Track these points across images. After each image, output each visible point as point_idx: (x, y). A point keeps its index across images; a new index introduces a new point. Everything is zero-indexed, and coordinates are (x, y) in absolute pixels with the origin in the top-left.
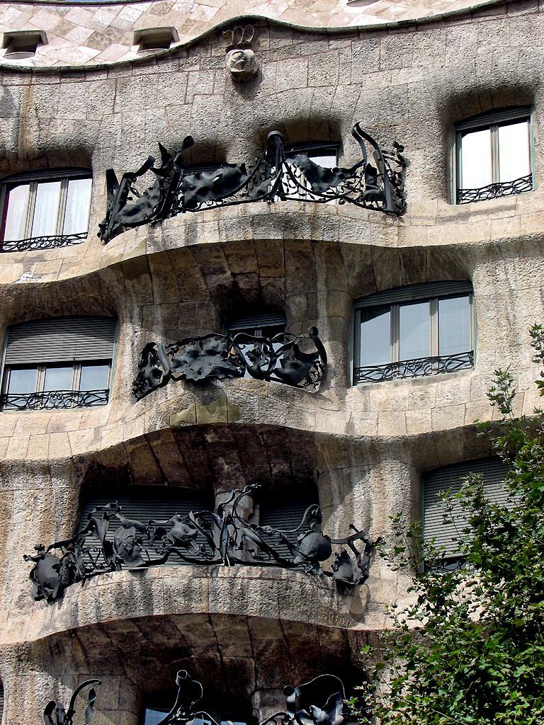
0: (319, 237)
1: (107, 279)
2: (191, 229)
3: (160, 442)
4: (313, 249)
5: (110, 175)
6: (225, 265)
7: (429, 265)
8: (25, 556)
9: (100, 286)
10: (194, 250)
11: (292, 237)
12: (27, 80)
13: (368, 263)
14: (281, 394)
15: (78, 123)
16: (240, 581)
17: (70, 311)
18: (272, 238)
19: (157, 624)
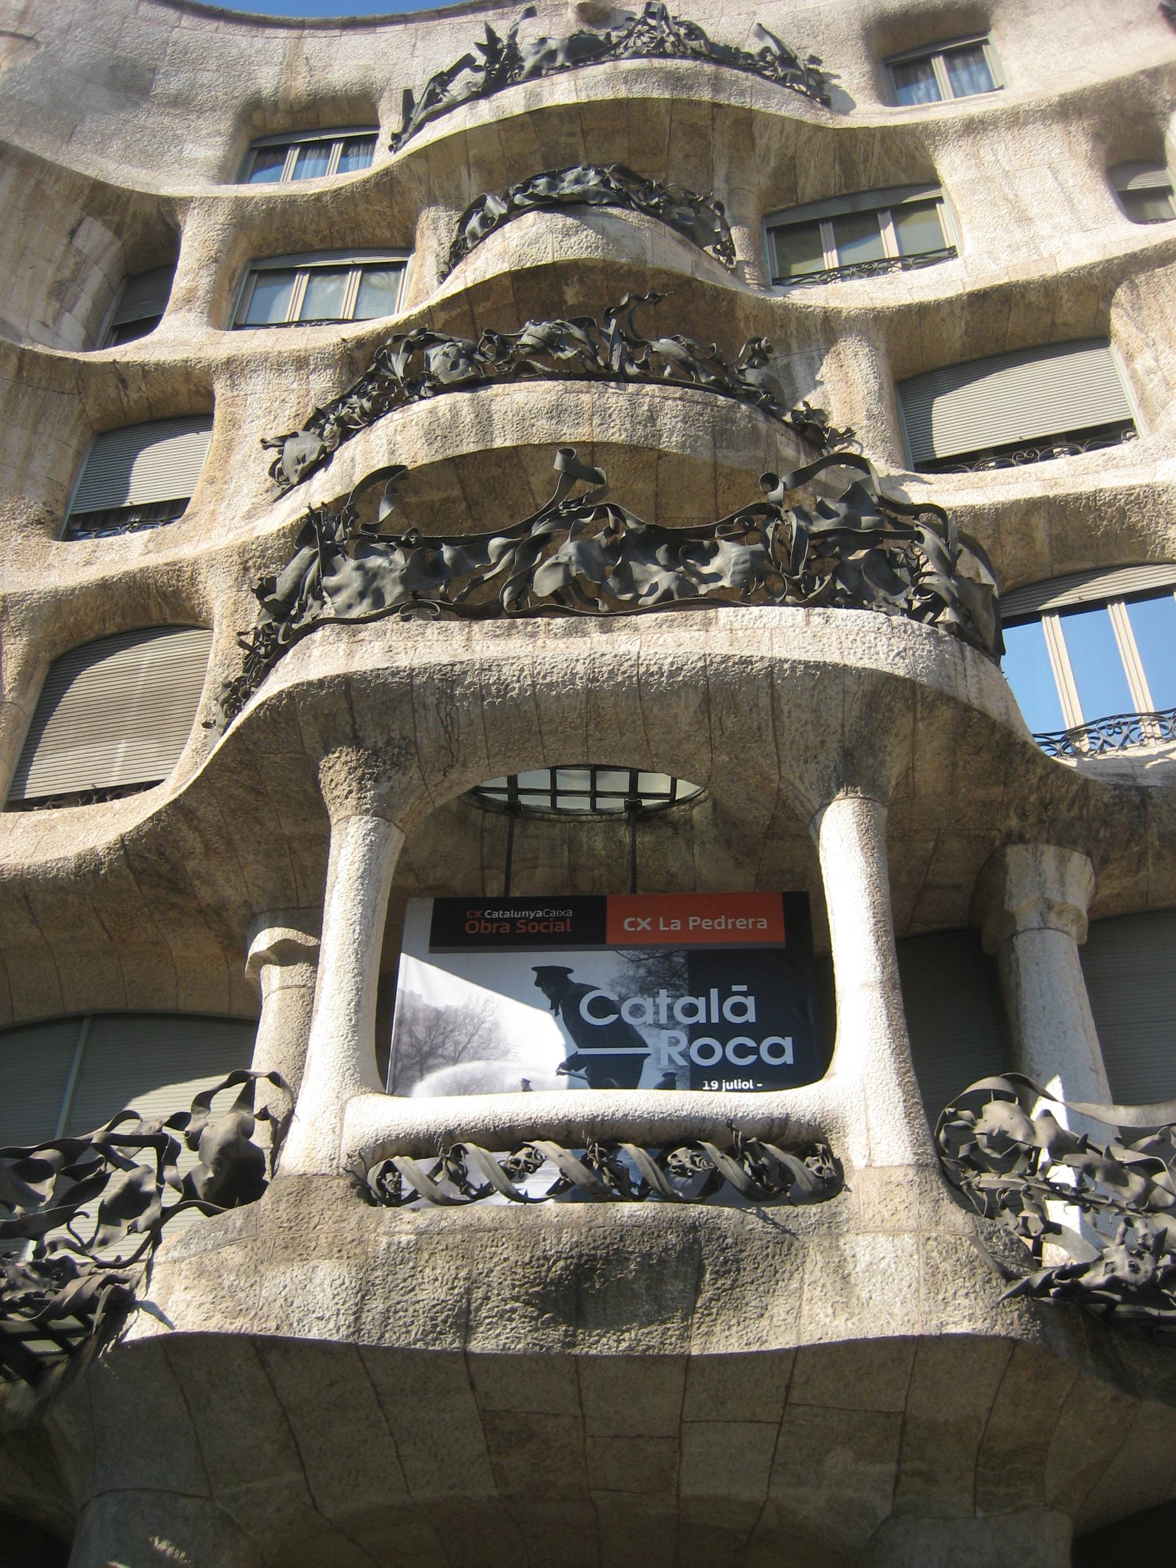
0: (722, 99)
1: (404, 179)
2: (533, 95)
3: (489, 305)
4: (713, 119)
5: (408, 94)
6: (581, 150)
7: (875, 161)
8: (263, 441)
9: (392, 190)
10: (539, 117)
11: (685, 96)
12: (295, 33)
13: (790, 152)
14: (681, 242)
15: (366, 67)
16: (647, 399)
17: (343, 239)
18: (655, 95)
19: (496, 471)
